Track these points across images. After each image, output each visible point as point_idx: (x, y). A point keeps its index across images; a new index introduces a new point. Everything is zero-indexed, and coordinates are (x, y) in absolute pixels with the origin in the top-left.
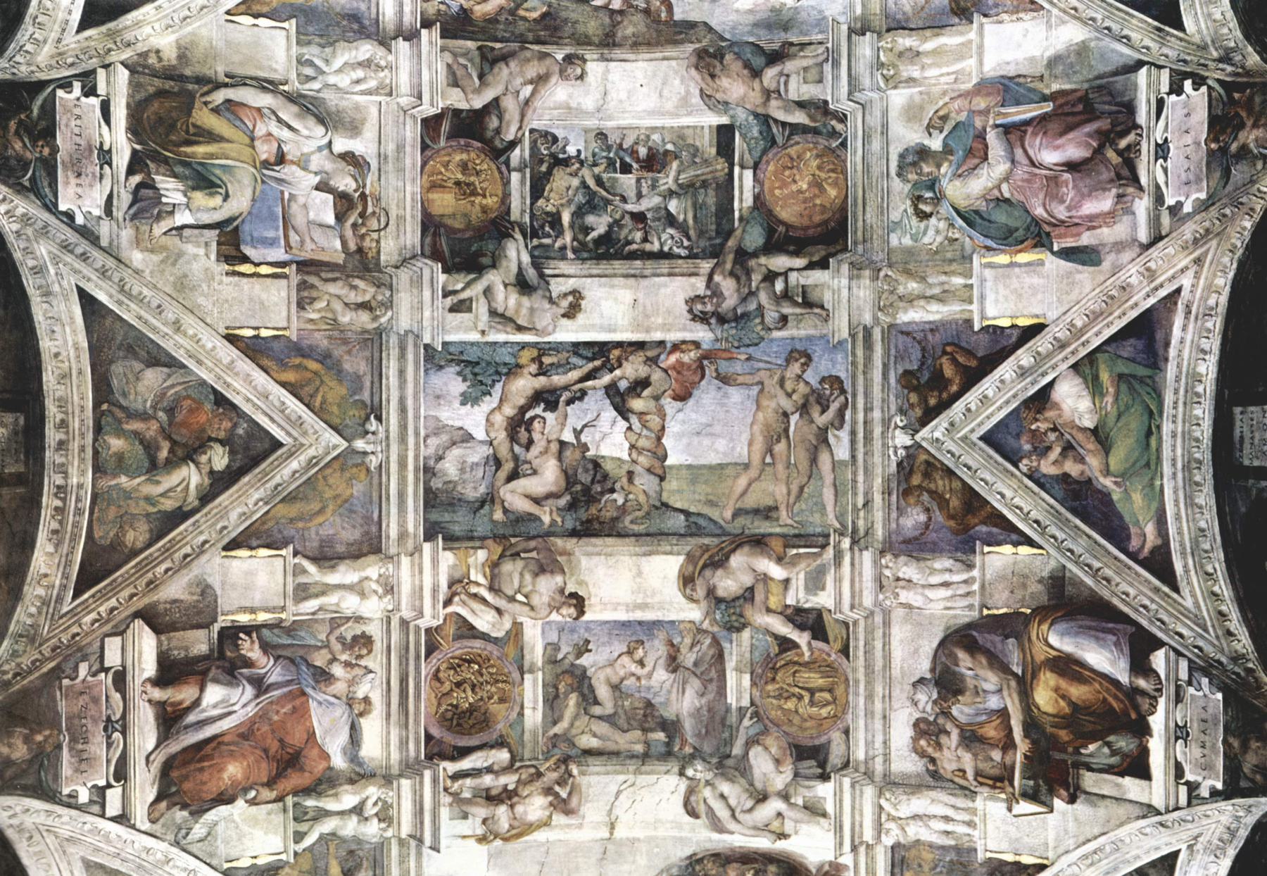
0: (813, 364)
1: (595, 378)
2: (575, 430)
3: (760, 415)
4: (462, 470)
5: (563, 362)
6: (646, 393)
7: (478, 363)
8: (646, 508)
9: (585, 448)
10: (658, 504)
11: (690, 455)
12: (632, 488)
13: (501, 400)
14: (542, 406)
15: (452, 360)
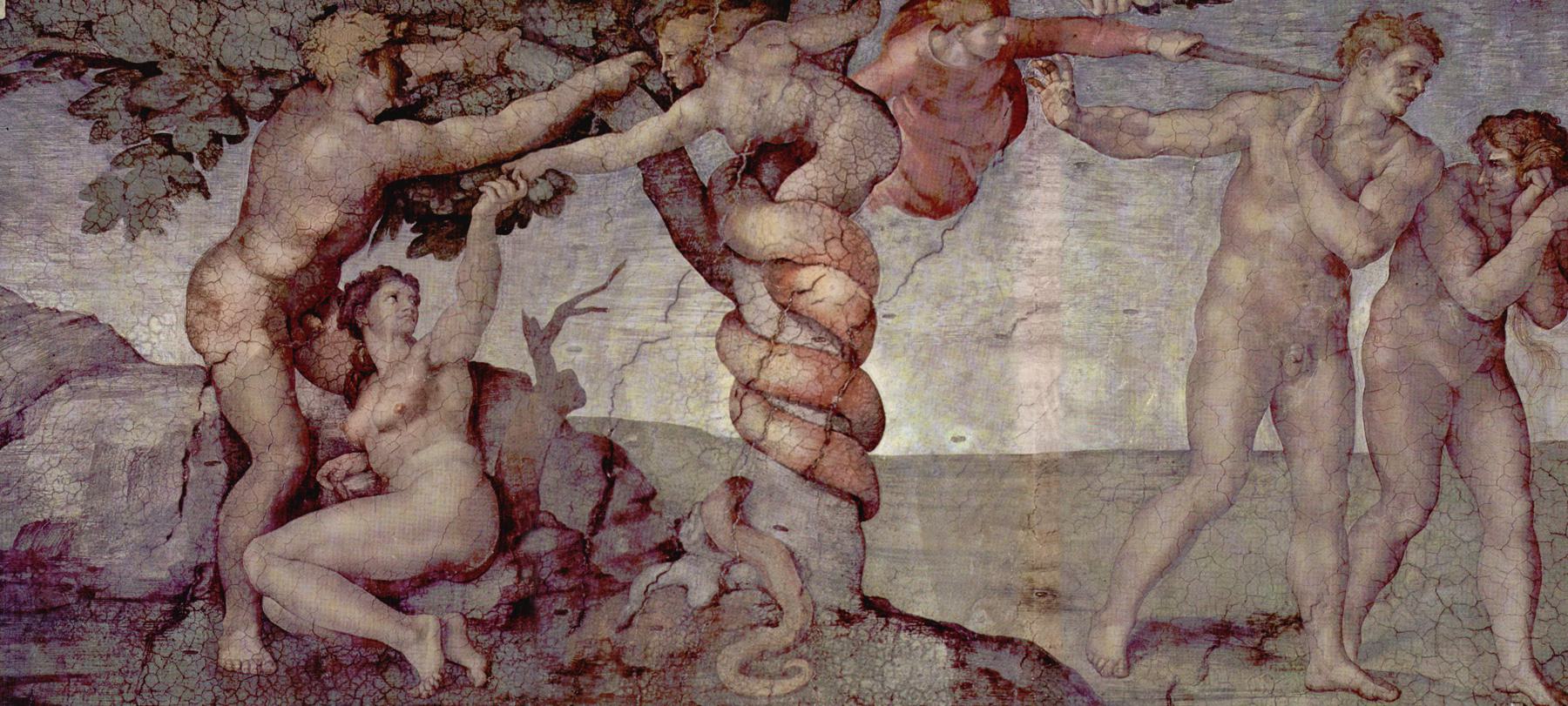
0: (1445, 71)
1: (604, 129)
2: (529, 326)
3: (1236, 271)
4: (96, 481)
5: (486, 66)
6: (798, 182)
7: (151, 70)
8: (794, 620)
9: (568, 391)
10: (853, 605)
11: (968, 419)
12: (745, 543)
13: (245, 210)
14: (407, 234)
15: (49, 57)
